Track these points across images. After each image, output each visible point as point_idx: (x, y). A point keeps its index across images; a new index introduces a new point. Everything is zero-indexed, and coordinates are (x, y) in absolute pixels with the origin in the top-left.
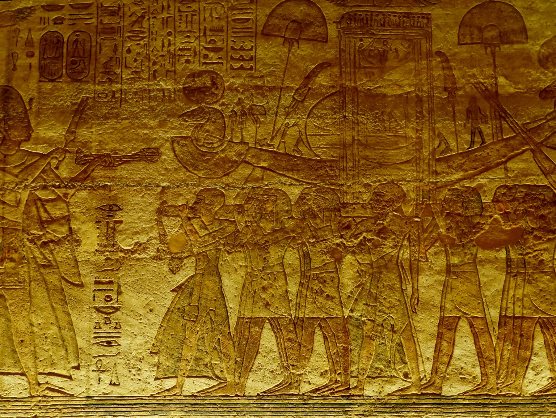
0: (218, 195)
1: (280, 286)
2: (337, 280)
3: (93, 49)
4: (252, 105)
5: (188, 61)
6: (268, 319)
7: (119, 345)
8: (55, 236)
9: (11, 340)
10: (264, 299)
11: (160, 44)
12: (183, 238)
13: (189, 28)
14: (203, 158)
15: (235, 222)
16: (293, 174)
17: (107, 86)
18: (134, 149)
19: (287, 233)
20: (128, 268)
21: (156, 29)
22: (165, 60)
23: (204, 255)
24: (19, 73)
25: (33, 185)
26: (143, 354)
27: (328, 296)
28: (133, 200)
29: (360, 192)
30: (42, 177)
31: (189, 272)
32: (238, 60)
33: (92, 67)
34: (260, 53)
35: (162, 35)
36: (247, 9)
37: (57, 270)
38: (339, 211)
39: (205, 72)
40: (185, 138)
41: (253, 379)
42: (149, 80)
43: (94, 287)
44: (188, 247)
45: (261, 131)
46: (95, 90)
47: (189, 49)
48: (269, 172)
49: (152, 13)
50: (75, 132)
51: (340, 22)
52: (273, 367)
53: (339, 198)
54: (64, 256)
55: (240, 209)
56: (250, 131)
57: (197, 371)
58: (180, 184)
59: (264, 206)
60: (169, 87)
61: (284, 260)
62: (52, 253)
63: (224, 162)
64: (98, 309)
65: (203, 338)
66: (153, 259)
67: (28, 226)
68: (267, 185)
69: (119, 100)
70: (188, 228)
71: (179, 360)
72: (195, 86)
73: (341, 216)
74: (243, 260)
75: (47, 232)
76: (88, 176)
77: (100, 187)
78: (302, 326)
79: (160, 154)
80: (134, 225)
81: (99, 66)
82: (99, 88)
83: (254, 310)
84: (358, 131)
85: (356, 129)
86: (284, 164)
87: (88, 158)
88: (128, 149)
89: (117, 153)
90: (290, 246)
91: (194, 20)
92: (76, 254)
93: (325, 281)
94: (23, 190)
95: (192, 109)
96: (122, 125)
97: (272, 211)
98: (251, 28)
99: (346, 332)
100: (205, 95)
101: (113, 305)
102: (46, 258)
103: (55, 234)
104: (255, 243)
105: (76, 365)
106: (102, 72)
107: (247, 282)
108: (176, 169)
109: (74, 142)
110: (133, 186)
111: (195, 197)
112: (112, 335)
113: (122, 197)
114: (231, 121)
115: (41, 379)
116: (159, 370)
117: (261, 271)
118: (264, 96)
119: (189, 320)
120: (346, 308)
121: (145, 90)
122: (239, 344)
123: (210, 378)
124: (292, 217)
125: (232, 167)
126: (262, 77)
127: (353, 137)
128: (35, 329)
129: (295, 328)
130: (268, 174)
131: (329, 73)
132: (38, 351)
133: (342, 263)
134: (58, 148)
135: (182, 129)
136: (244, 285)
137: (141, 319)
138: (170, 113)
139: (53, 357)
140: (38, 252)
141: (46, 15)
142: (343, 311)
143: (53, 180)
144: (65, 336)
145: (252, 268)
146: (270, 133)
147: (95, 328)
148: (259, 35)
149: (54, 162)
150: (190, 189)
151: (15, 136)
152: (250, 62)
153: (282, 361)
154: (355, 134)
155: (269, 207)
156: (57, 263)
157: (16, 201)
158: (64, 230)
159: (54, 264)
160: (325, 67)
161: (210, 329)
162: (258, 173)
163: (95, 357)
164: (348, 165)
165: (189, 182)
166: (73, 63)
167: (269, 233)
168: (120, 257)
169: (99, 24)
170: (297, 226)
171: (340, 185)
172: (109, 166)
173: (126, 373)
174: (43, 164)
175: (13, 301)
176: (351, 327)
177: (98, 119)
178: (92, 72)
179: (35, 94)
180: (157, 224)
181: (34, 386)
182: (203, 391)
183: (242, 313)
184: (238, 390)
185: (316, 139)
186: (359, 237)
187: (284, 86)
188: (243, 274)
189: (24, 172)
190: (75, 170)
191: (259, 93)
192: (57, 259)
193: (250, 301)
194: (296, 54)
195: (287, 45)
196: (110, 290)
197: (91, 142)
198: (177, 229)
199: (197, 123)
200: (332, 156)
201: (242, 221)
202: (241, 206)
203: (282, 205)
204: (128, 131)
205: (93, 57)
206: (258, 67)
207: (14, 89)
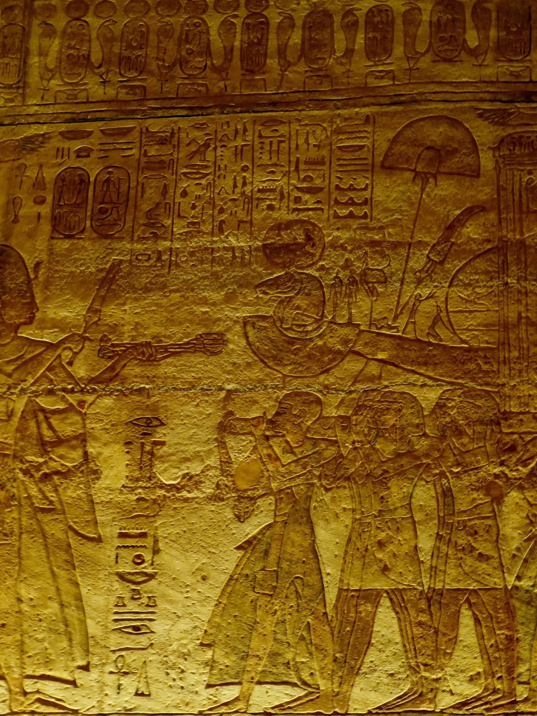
0: (312, 402)
1: (405, 540)
2: (494, 530)
3: (132, 192)
4: (365, 270)
6: (386, 591)
7: (152, 632)
10: (381, 561)
11: (231, 183)
12: (257, 467)
13: (274, 160)
14: (290, 346)
15: (336, 442)
16: (427, 370)
17: (149, 244)
18: (187, 335)
19: (417, 458)
20: (171, 512)
21: (225, 162)
22: (236, 206)
23: (288, 493)
25: (34, 388)
26: (190, 647)
27: (480, 554)
28: (182, 411)
29: (530, 395)
30: (47, 377)
31: (265, 519)
32: (346, 204)
33: (129, 218)
34: (379, 194)
35: (234, 171)
36: (359, 132)
37: (62, 516)
38: (498, 424)
39: (297, 222)
40: (263, 318)
41: (361, 686)
42: (212, 234)
43: (118, 542)
44: (264, 480)
45: (379, 307)
46: (132, 250)
47: (273, 190)
48: (390, 367)
49: (221, 140)
50: (100, 311)
51: (498, 148)
52: (394, 667)
53: (498, 404)
54: (74, 495)
55: (345, 423)
56: (362, 308)
57: (274, 674)
58: (255, 386)
59: (382, 418)
60: (242, 244)
61: (413, 500)
62: (56, 491)
63: (322, 353)
64: (122, 577)
65: (284, 622)
66: (210, 499)
67: (23, 449)
68: (386, 387)
69: (167, 264)
70: (265, 452)
71: (245, 657)
72: (280, 242)
73: (501, 432)
74: (349, 501)
75: (51, 458)
76: (117, 375)
77: (133, 391)
78: (440, 603)
79: (225, 342)
80: (183, 448)
81: (140, 215)
82: (138, 246)
83: (364, 577)
84: (527, 305)
85: (524, 302)
86: (413, 355)
87: (117, 349)
88: (178, 334)
89: (161, 341)
90: (422, 479)
91: (281, 148)
92: (93, 492)
93: (476, 533)
95: (275, 275)
96: (170, 300)
97: (394, 425)
98: (366, 159)
99: (510, 611)
100: (295, 255)
101: (145, 570)
103: (62, 462)
104: (368, 475)
106: (144, 225)
107: (354, 534)
108: (249, 364)
109: (98, 325)
110: (184, 389)
111: (278, 404)
112: (142, 616)
113: (166, 406)
114: (333, 292)
116: (214, 672)
117: (376, 517)
118: (384, 256)
119: (264, 594)
120: (510, 574)
121: (206, 249)
122: (339, 632)
123: (295, 685)
124: (425, 435)
125: (334, 359)
126: (381, 228)
127: (520, 314)
129: (429, 606)
130: (389, 370)
131: (482, 220)
133: (504, 505)
135: (260, 305)
136: (349, 540)
137: (188, 592)
138: (242, 281)
141: (66, 144)
142: (504, 579)
143: (64, 381)
145: (363, 512)
146: (392, 309)
147: (116, 606)
148: (377, 169)
149: (67, 355)
150: (269, 393)
151: (12, 317)
152: (363, 207)
153: (407, 658)
154: (522, 308)
155: (390, 419)
156: (62, 505)
158: (77, 455)
159: (59, 507)
160: (476, 213)
161: (295, 608)
162: (373, 369)
163: (114, 651)
164: (512, 355)
165: (269, 383)
166: (102, 211)
167: (390, 459)
168: (159, 496)
169: (142, 156)
170: (432, 447)
171: (499, 385)
172: (148, 360)
173: (161, 676)
174: (50, 358)
176: (517, 604)
177: (135, 292)
178: (129, 224)
179: (44, 257)
180: (218, 446)
182: (281, 705)
183: (346, 582)
184: (338, 704)
185: (463, 318)
186: (530, 464)
187: (414, 241)
188: (348, 522)
189: (22, 369)
190: (97, 367)
191: (377, 251)
192: (64, 498)
193: (358, 564)
194: (432, 195)
195: (419, 181)
196: (141, 546)
197: (123, 325)
198: (248, 454)
199: (283, 296)
200: (487, 342)
201: (347, 442)
202: (346, 418)
203: (409, 417)
204: (178, 309)
205: (131, 203)
206: (375, 214)
207: (13, 249)
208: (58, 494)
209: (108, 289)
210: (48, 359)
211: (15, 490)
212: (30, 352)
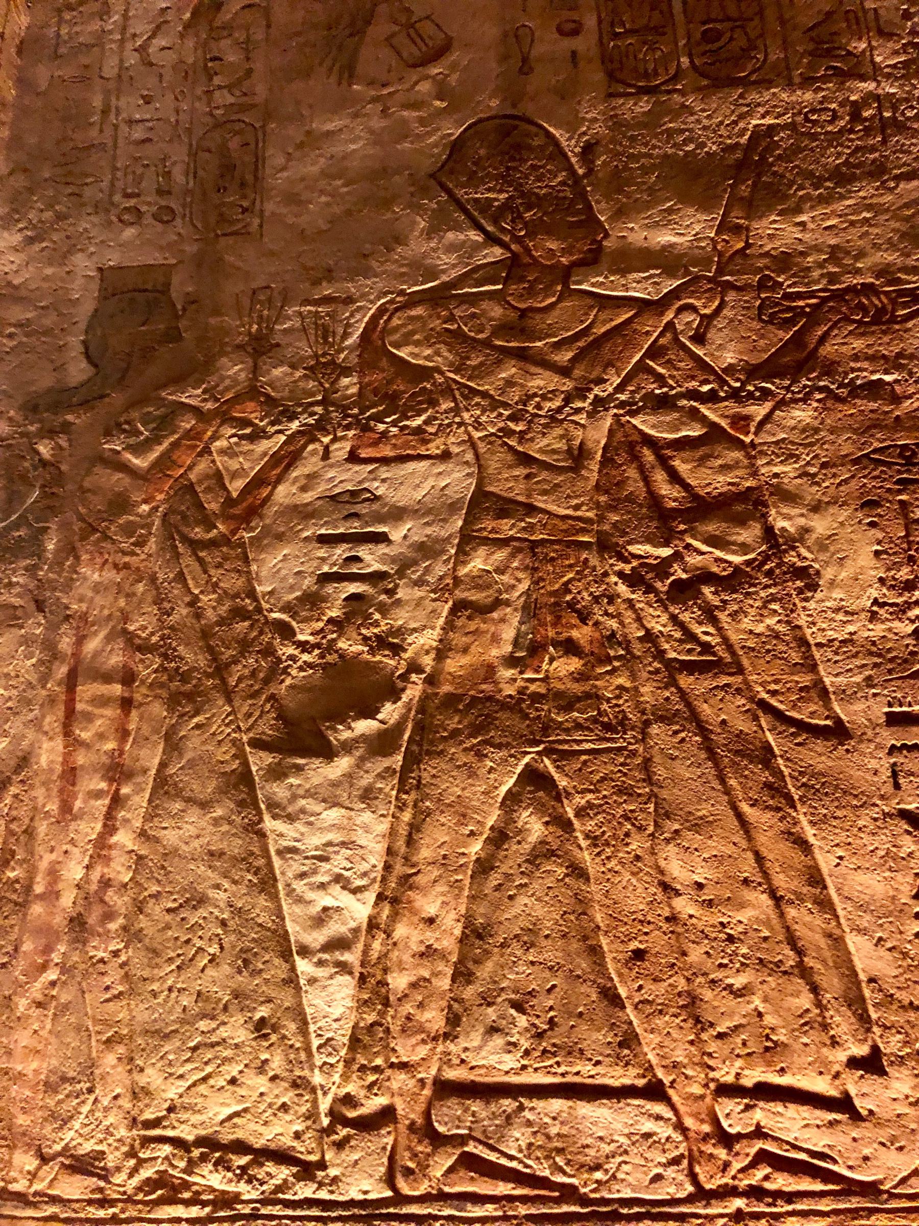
8: (718, 560)
9: (595, 951)
24: (543, 78)
25: (623, 397)
30: (651, 371)
37: (739, 679)
43: (889, 737)
50: (748, 229)
54: (760, 628)
62: (714, 621)
75: (688, 546)
77: (855, 391)
89: (899, 281)
92: (802, 621)
94: (591, 415)
102: (690, 636)
103: (718, 553)
105: (862, 1050)
115: (733, 1116)
128: (684, 906)
132: (708, 994)
134: (696, 279)
139: (769, 1020)
140: (664, 618)
143: (693, 378)
144: (800, 930)
156: (733, 653)
157: (569, 451)
172: (876, 321)
174: (652, 329)
175: (590, 796)
181: (709, 1149)
192: (734, 637)
197: (802, 254)
208: (720, 629)
209: (755, 184)
210: (648, 333)
211: (613, 624)
212: (604, 322)
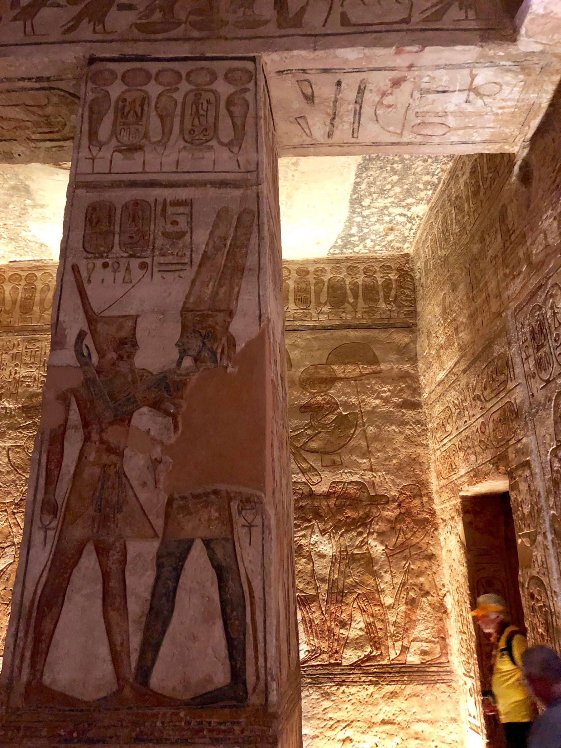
5: (28, 386)
11: (9, 373)
13: (32, 360)
22: (10, 385)
47: (30, 377)
108: (8, 472)
